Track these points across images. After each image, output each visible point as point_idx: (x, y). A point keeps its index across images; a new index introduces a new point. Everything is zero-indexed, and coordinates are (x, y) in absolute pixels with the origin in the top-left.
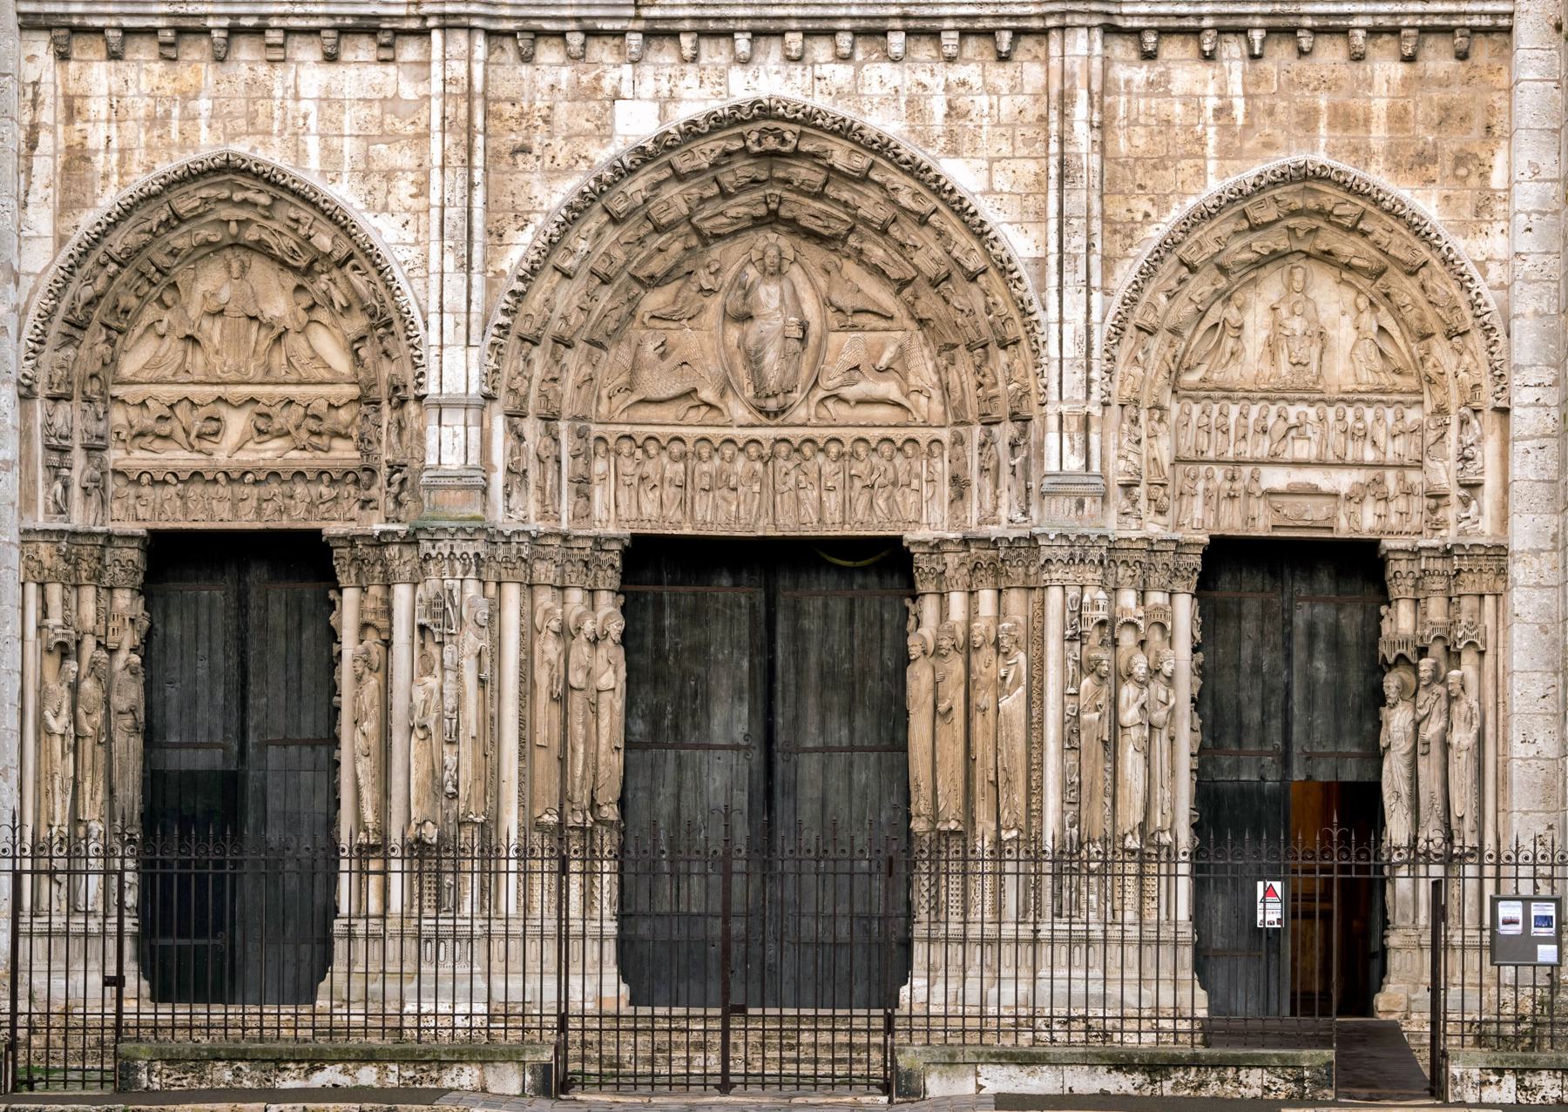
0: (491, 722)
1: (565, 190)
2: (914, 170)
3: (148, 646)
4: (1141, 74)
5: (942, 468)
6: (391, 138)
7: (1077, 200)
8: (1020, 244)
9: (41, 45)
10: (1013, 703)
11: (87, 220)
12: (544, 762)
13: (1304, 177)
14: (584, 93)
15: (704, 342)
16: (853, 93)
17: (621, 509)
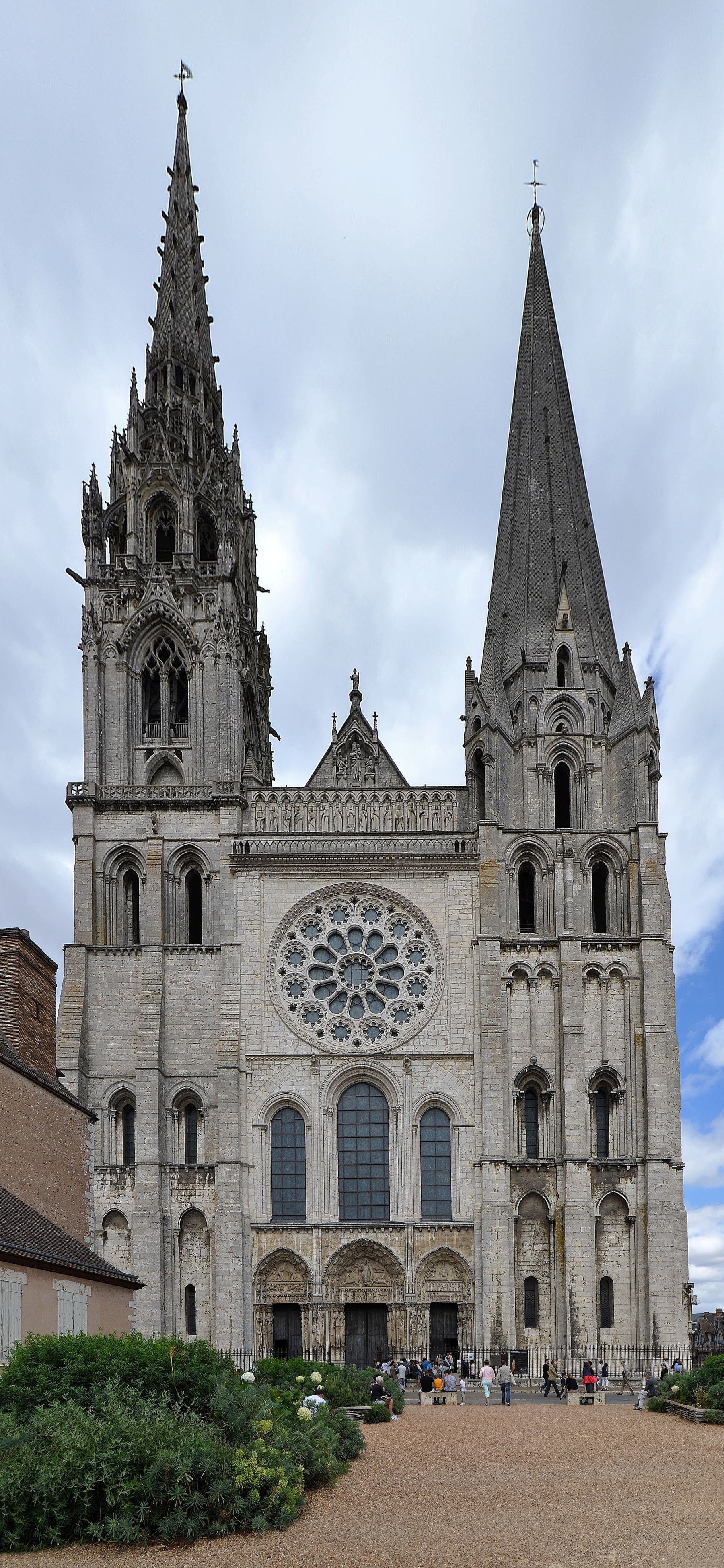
0: (325, 1332)
1: (334, 1252)
2: (386, 1248)
3: (273, 1321)
4: (419, 1234)
5: (392, 1293)
6: (307, 1244)
7: (410, 1252)
8: (401, 1259)
9: (255, 1232)
10: (402, 1328)
11: (262, 1257)
12: (333, 1338)
13: (444, 1249)
14: (335, 1238)
15: (355, 1276)
16: (376, 1237)
17: (344, 1300)
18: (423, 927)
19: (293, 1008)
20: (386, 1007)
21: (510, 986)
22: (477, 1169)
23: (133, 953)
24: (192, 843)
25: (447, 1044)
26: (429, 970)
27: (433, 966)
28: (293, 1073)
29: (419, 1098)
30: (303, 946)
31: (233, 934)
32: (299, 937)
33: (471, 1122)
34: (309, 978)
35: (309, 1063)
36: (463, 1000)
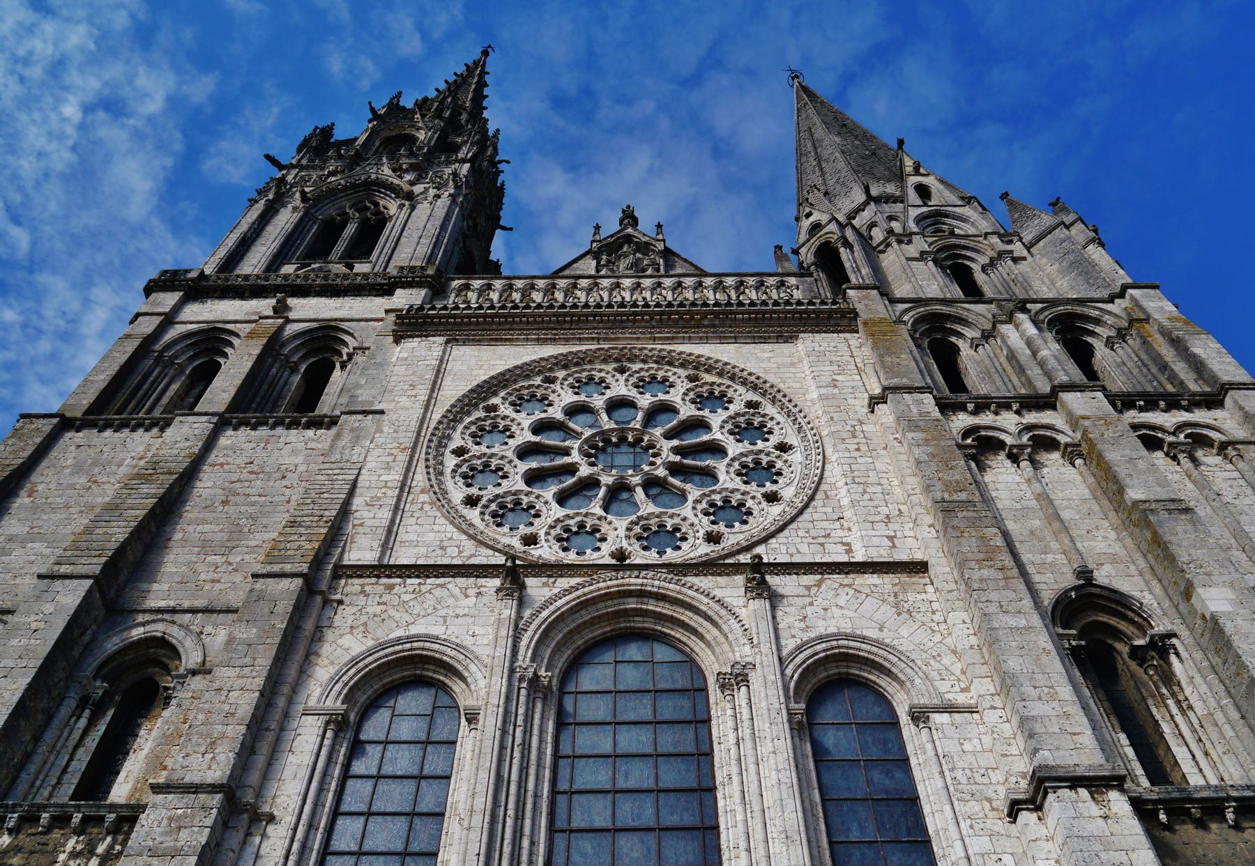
18: (764, 395)
19: (471, 502)
20: (691, 498)
21: (973, 457)
22: (1026, 817)
23: (155, 430)
24: (333, 324)
25: (849, 551)
26: (783, 448)
27: (793, 439)
28: (451, 601)
29: (799, 649)
30: (513, 420)
31: (372, 403)
32: (506, 410)
33: (961, 699)
34: (516, 460)
35: (497, 582)
36: (871, 480)
